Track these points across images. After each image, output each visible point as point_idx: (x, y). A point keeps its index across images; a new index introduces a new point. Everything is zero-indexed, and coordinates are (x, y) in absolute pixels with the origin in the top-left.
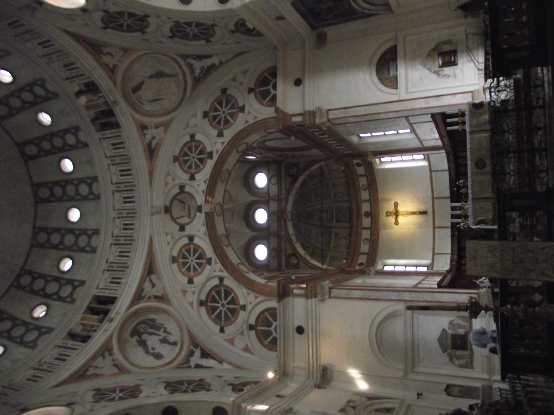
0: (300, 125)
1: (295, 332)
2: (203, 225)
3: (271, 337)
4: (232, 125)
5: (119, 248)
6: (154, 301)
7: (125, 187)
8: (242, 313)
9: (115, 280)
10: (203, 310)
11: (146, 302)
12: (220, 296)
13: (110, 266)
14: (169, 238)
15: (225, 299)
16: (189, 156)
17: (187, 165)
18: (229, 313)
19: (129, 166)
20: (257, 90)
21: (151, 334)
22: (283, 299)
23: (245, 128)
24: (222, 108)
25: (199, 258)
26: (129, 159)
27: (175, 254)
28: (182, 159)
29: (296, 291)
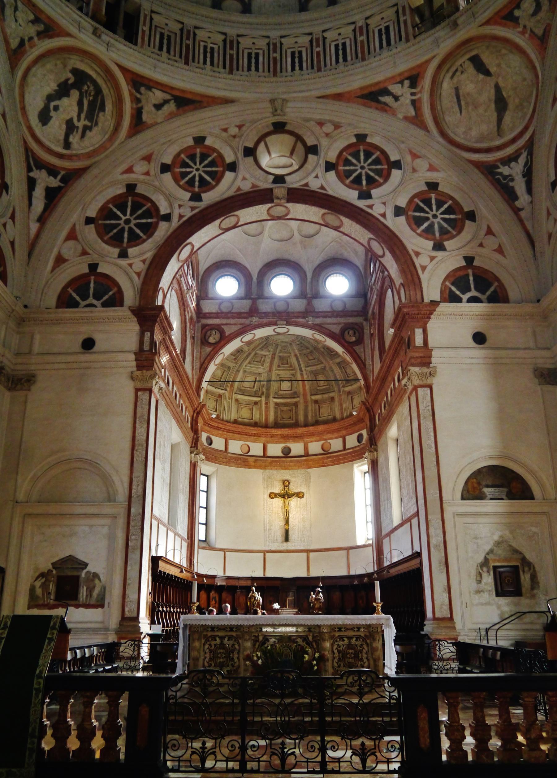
0: (410, 342)
1: (86, 336)
2: (254, 186)
3: (78, 298)
4: (414, 231)
5: (219, 47)
6: (132, 108)
8: (116, 251)
9: (165, 41)
10: (121, 190)
11: (131, 94)
13: (189, 32)
14: (234, 131)
15: (138, 225)
16: (366, 160)
17: (350, 158)
18: (115, 231)
19: (352, 59)
20: (470, 271)
21: (80, 104)
22: (134, 314)
23: (408, 252)
24: (442, 214)
25: (201, 178)
26: (363, 59)
27: (208, 142)
29: (147, 335)
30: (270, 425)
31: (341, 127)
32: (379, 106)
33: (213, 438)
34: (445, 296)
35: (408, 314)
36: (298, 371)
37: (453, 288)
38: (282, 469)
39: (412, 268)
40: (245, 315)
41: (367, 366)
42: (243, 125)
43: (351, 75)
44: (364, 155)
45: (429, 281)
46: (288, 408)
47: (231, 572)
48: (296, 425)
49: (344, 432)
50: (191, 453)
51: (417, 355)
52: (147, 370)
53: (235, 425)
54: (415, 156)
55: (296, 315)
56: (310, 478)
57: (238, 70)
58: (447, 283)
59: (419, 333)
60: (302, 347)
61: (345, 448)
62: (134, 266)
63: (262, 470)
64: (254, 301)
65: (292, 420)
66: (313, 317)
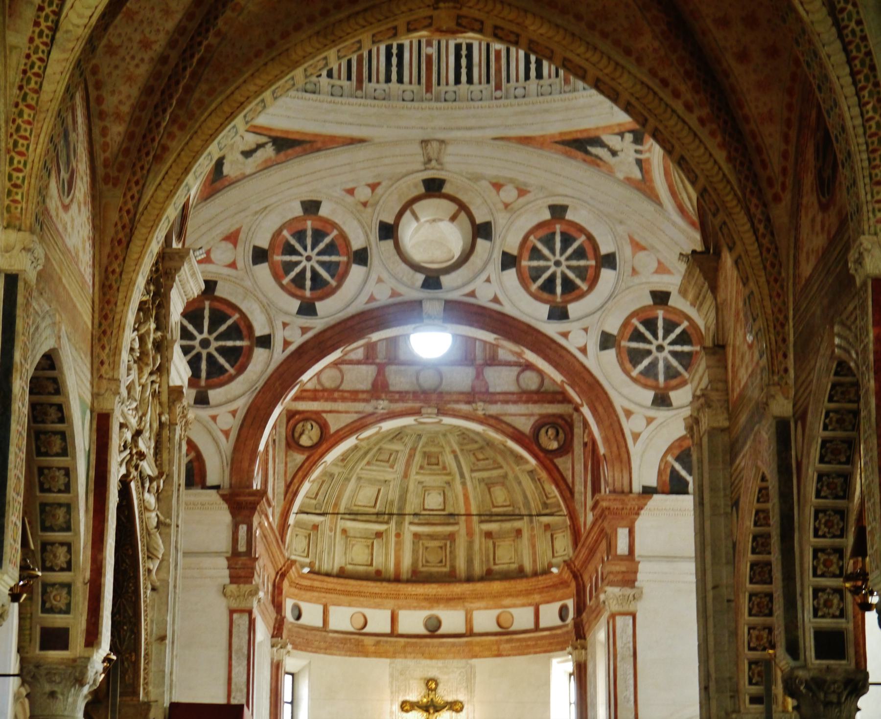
0: (611, 547)
4: (628, 373)
7: (498, 53)
14: (363, 193)
15: (222, 350)
16: (563, 250)
17: (540, 246)
19: (550, 76)
23: (615, 411)
24: (671, 343)
27: (324, 212)
28: (558, 228)
29: (243, 529)
30: (405, 575)
31: (529, 192)
32: (588, 158)
33: (304, 606)
34: (664, 478)
35: (609, 509)
36: (458, 477)
37: (678, 467)
38: (425, 658)
39: (619, 437)
40: (364, 396)
41: (577, 496)
42: (379, 184)
43: (546, 111)
44: (562, 241)
45: (642, 456)
46: (436, 543)
48: (450, 578)
49: (537, 598)
50: (273, 646)
51: (617, 568)
52: (246, 583)
53: (342, 581)
54: (637, 247)
55: (455, 397)
56: (475, 677)
57: (370, 80)
58: (670, 459)
59: (622, 535)
60: (464, 439)
61: (537, 628)
62: (218, 419)
63: (388, 661)
64: (381, 369)
65: (445, 566)
66: (484, 401)
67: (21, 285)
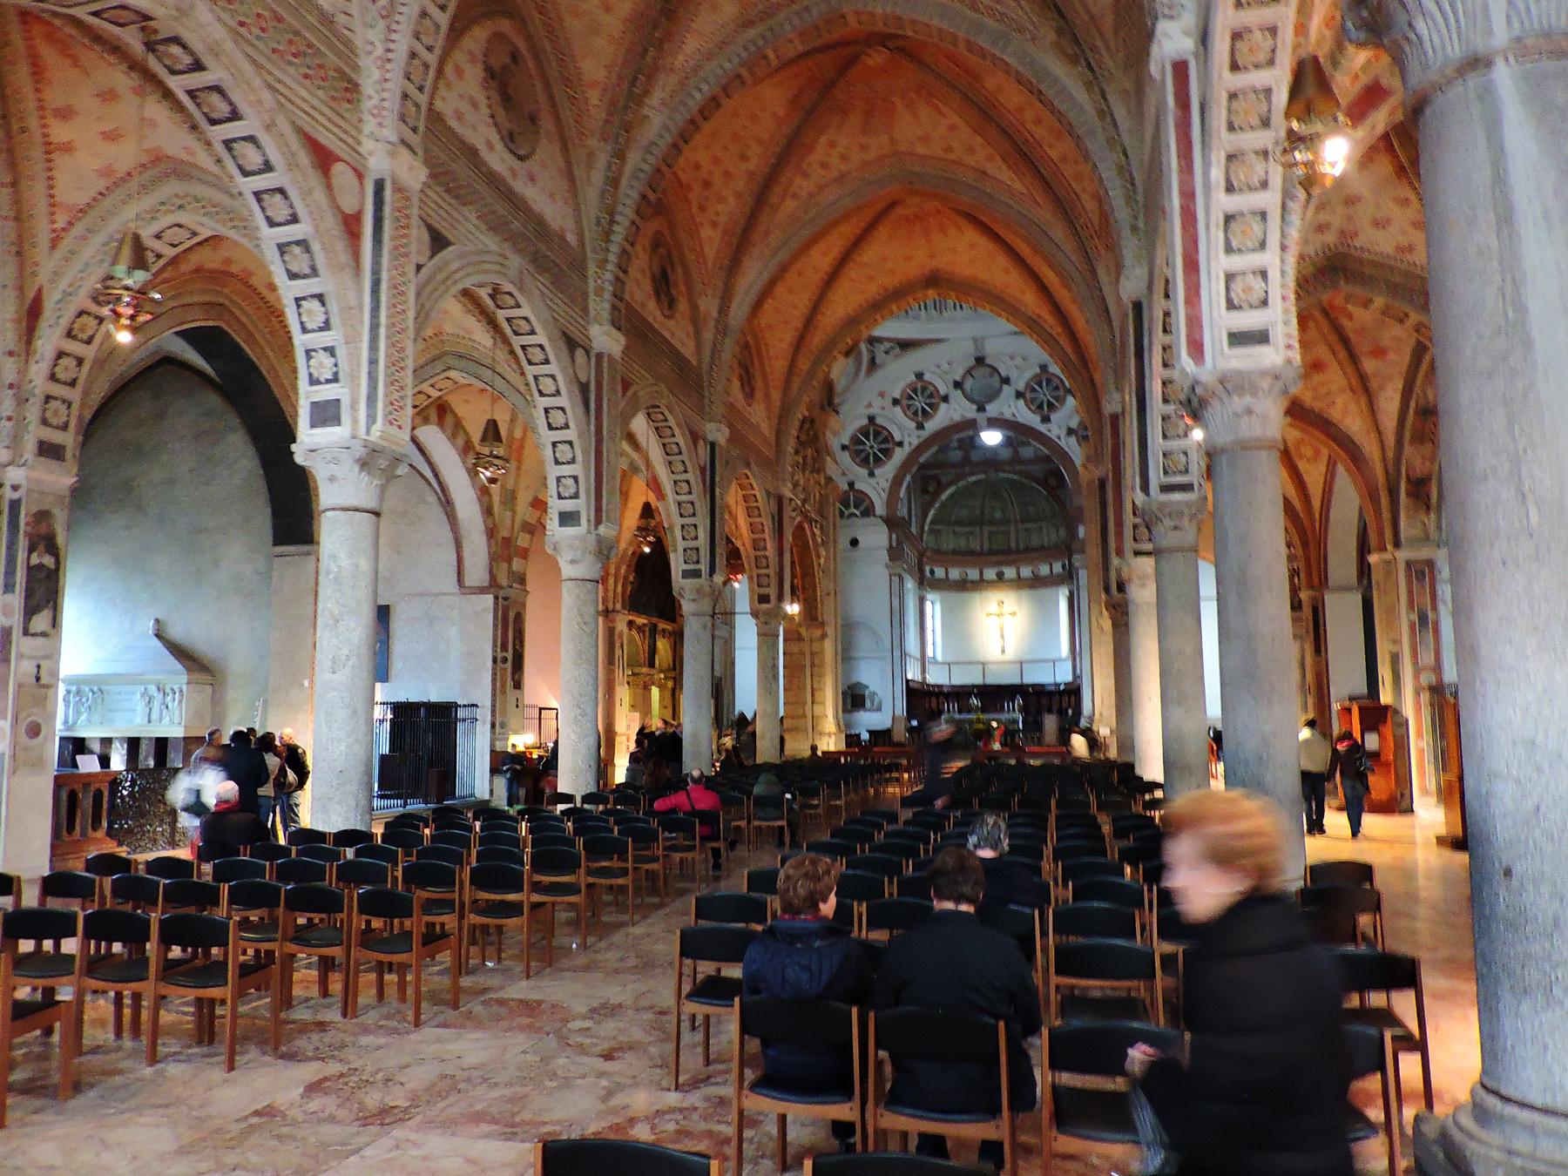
10: (865, 422)
12: (882, 442)
14: (945, 366)
27: (927, 377)
47: (956, 681)
48: (1008, 552)
67: (717, 449)
